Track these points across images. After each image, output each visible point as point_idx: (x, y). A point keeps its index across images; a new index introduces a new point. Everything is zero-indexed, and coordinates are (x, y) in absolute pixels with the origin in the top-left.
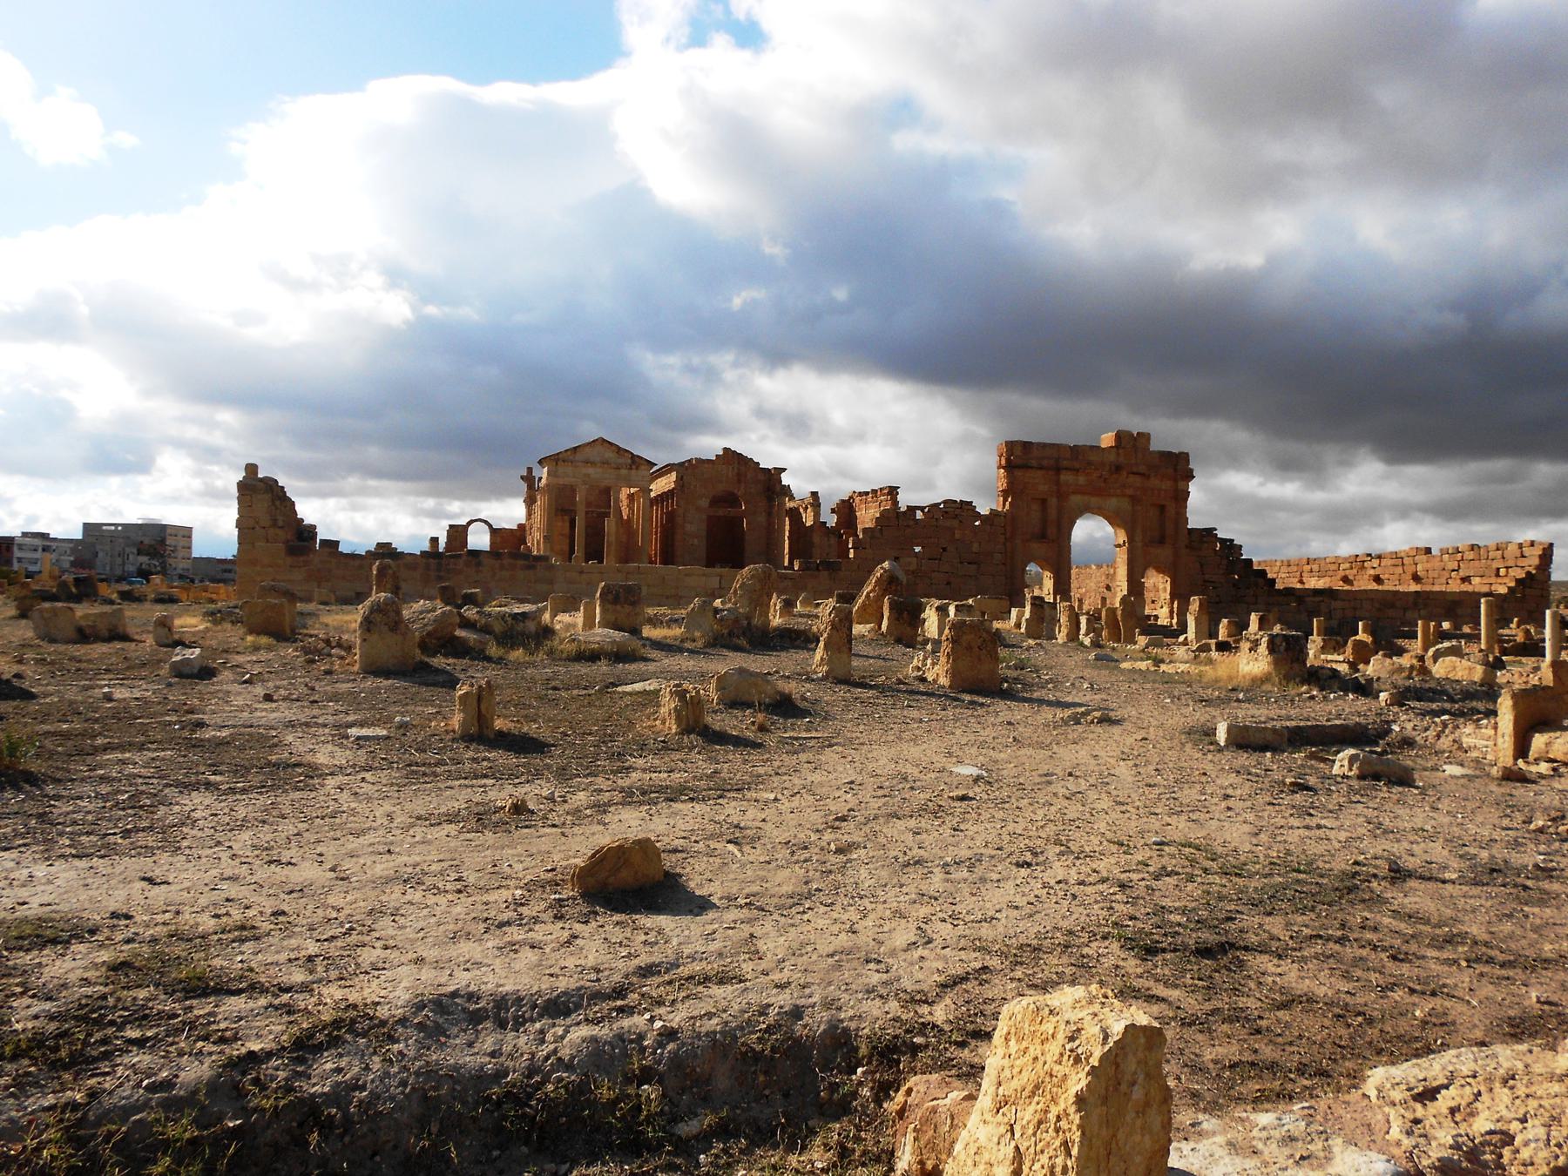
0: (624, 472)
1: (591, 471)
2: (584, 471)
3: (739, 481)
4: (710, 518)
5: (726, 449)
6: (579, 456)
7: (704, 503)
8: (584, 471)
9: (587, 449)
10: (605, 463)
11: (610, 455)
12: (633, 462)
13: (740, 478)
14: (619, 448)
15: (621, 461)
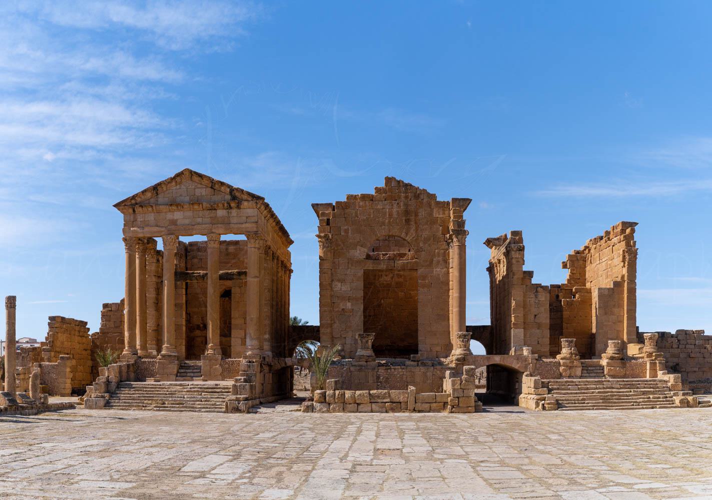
0: (221, 213)
1: (178, 215)
2: (169, 216)
3: (408, 221)
4: (367, 274)
5: (389, 180)
6: (161, 199)
7: (359, 253)
8: (169, 216)
9: (173, 186)
10: (195, 202)
11: (203, 192)
12: (234, 198)
13: (408, 216)
14: (211, 180)
15: (217, 198)
